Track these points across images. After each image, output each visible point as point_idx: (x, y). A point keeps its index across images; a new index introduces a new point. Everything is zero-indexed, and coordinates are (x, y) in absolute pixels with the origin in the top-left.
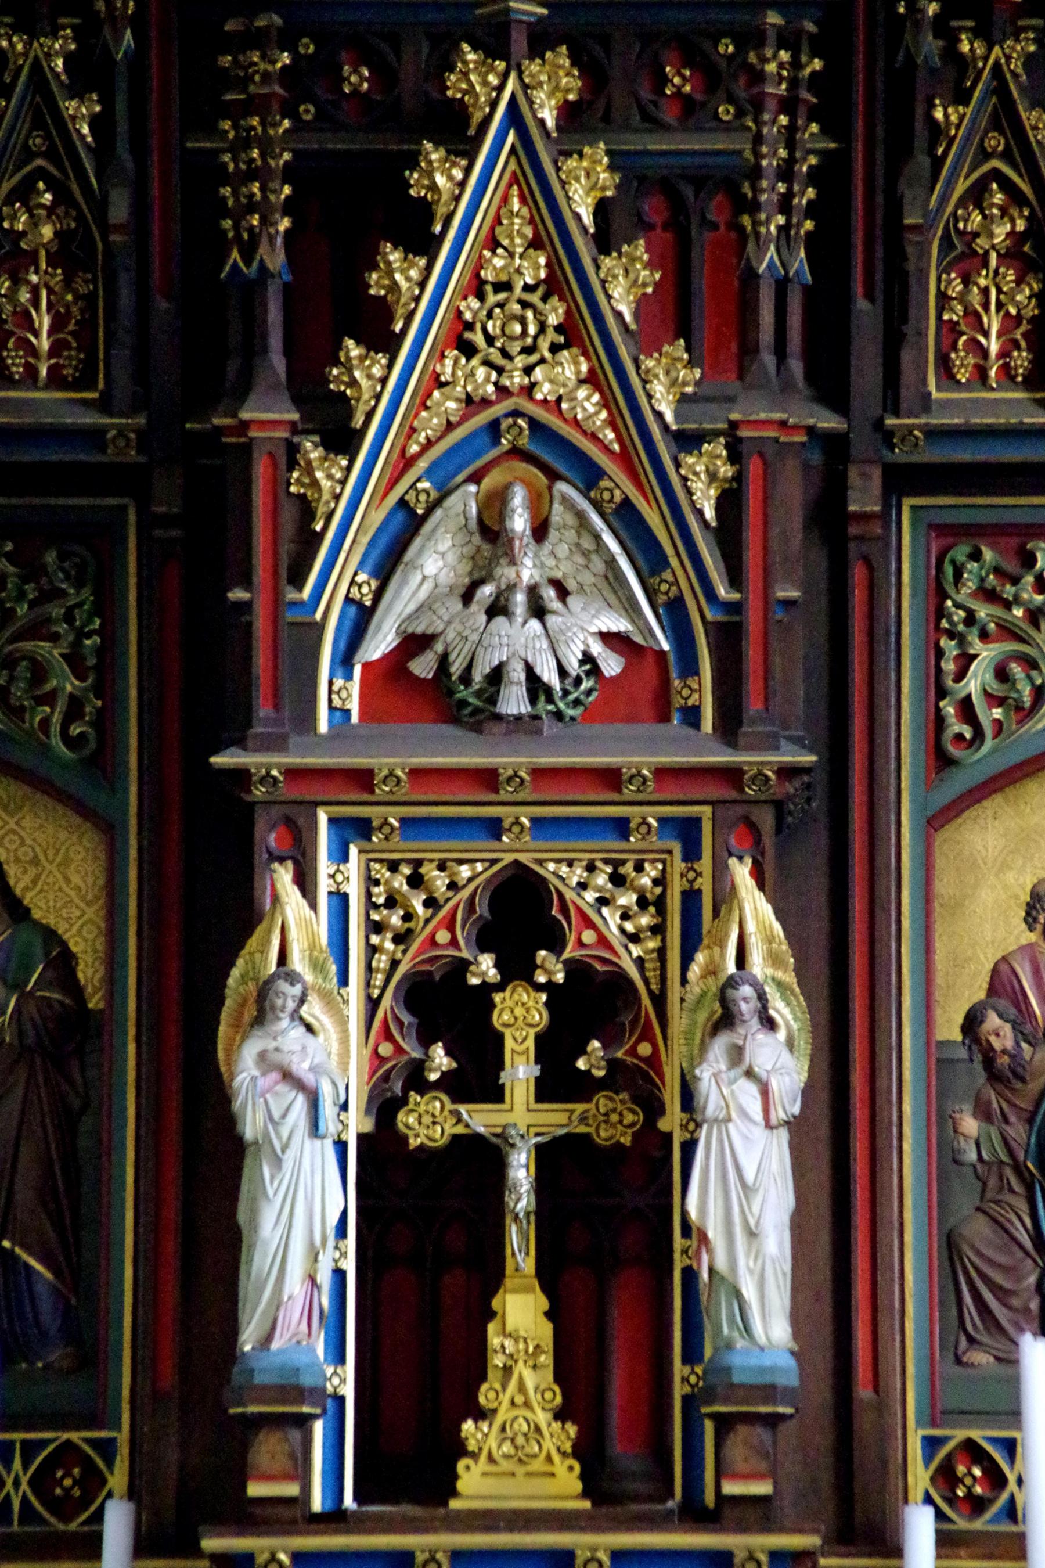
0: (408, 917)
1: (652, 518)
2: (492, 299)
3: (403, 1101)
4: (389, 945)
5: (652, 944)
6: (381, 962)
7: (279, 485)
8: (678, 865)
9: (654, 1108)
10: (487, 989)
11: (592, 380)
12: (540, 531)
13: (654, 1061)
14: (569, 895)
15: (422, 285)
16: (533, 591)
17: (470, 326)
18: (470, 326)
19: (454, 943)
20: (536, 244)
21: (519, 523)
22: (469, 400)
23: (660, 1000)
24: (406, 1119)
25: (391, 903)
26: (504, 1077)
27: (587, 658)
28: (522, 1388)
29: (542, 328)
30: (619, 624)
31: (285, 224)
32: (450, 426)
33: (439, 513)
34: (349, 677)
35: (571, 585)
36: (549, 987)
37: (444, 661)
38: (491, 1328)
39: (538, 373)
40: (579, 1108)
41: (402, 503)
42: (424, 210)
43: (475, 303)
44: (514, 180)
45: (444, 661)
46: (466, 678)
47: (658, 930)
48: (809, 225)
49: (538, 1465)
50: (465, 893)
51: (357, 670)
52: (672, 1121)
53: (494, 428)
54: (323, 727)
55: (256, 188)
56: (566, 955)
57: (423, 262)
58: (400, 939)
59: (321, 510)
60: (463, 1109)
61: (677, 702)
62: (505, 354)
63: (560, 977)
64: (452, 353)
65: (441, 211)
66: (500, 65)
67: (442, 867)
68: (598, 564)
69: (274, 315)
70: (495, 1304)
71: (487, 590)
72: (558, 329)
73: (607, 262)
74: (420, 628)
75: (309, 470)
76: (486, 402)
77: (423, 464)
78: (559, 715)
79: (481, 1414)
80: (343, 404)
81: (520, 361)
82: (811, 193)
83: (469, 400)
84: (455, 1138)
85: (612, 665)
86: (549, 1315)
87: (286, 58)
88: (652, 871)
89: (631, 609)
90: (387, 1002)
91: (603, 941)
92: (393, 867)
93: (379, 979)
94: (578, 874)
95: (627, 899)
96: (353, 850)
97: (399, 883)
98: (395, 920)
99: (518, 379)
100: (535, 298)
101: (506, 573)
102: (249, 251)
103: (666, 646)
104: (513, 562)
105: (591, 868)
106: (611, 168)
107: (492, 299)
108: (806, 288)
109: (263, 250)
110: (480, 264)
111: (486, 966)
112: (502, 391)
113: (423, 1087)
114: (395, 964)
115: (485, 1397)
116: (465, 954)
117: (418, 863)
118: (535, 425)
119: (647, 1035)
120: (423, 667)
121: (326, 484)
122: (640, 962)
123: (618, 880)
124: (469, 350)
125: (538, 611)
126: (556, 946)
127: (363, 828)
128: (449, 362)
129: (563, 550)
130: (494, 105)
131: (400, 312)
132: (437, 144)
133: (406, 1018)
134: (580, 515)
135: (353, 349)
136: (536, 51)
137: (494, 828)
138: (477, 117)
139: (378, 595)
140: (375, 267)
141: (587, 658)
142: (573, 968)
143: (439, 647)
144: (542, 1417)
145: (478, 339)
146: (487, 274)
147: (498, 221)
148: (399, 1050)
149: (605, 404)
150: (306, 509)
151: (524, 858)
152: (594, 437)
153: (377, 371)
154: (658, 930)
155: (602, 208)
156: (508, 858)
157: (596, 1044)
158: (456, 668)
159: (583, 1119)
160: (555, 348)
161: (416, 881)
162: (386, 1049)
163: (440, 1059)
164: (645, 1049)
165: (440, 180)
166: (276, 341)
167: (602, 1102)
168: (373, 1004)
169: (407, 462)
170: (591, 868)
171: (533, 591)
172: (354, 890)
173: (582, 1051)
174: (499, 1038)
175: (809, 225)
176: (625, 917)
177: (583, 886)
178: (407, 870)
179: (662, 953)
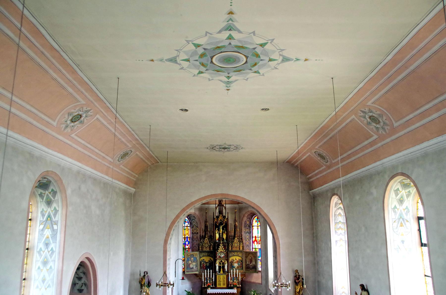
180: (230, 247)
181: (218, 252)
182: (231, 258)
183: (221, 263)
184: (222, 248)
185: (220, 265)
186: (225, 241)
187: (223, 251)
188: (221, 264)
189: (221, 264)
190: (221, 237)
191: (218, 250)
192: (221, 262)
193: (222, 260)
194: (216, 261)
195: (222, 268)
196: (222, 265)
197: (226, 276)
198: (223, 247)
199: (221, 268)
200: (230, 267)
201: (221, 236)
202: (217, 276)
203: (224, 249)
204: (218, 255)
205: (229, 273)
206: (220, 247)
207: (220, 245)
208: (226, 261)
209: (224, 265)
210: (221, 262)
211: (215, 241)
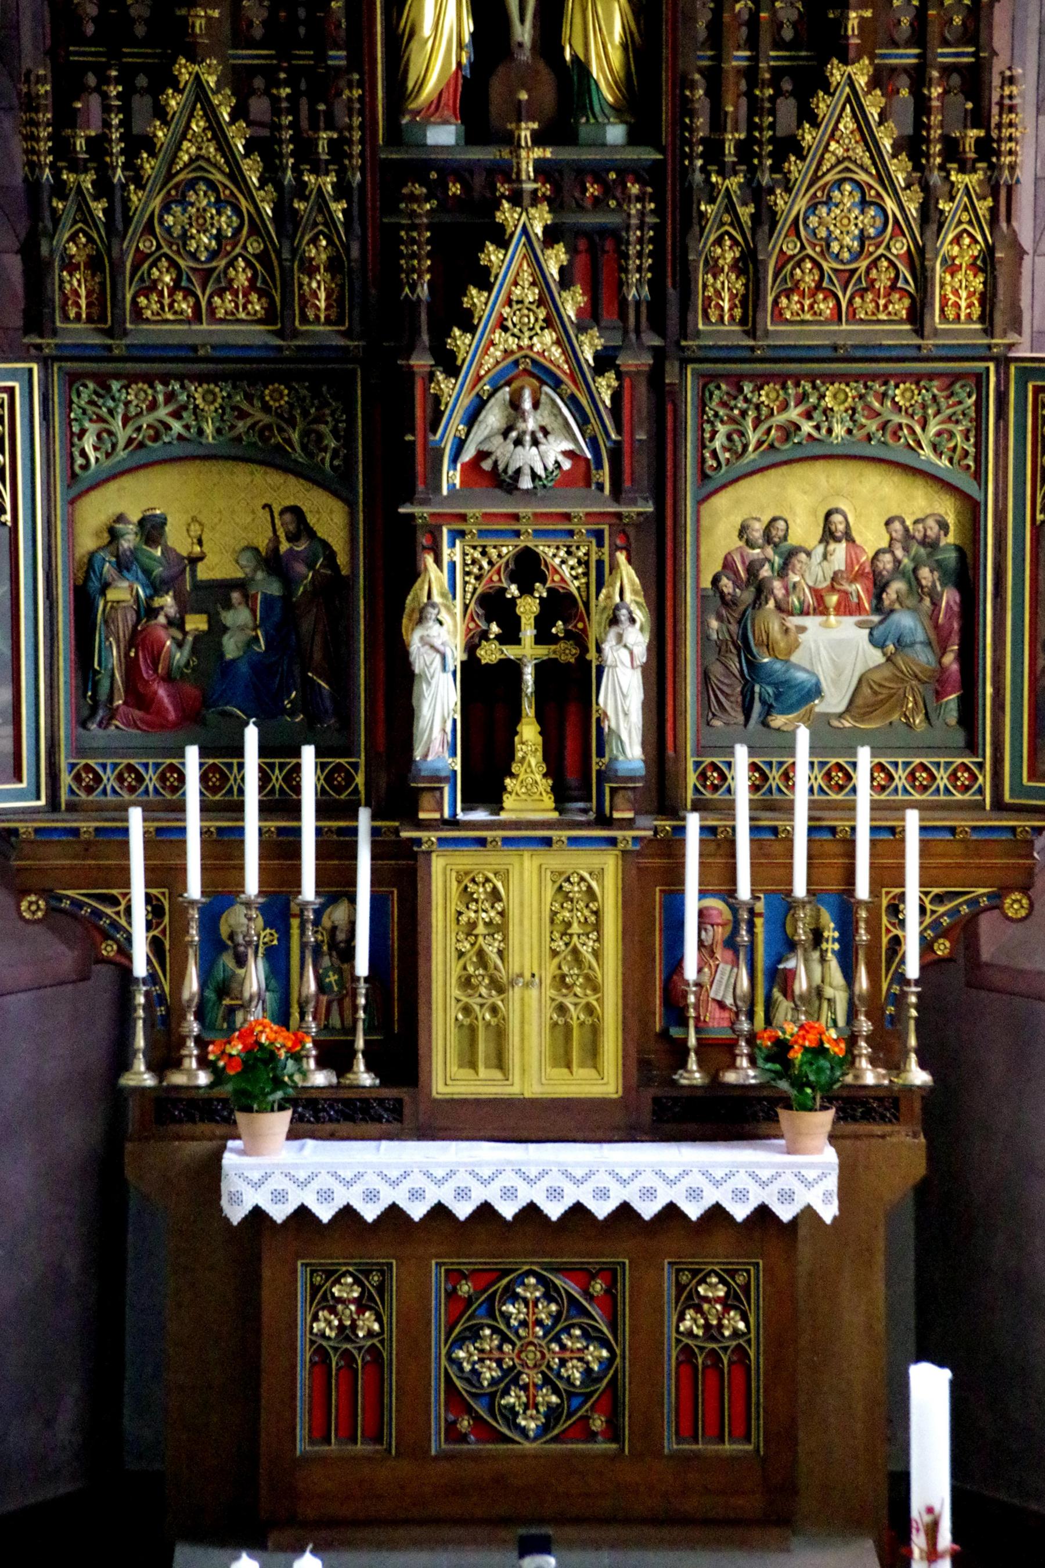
0: (481, 568)
1: (584, 401)
2: (515, 307)
3: (479, 645)
4: (473, 581)
5: (583, 580)
6: (470, 588)
7: (426, 389)
8: (594, 548)
9: (585, 650)
10: (514, 598)
11: (558, 342)
12: (536, 405)
13: (584, 630)
14: (549, 560)
15: (486, 304)
16: (533, 433)
17: (506, 319)
18: (506, 319)
19: (500, 580)
20: (533, 284)
21: (527, 405)
22: (505, 351)
23: (587, 604)
24: (480, 653)
25: (474, 562)
26: (521, 635)
27: (557, 462)
28: (530, 765)
29: (536, 320)
30: (569, 446)
31: (428, 277)
32: (498, 363)
33: (493, 400)
34: (455, 469)
35: (549, 428)
36: (541, 598)
37: (496, 463)
38: (517, 739)
39: (535, 339)
40: (553, 647)
41: (478, 395)
42: (487, 270)
43: (507, 309)
44: (525, 256)
45: (496, 463)
46: (505, 471)
47: (586, 574)
48: (649, 275)
49: (536, 797)
50: (504, 560)
51: (459, 466)
52: (592, 655)
53: (516, 363)
54: (445, 492)
55: (415, 262)
56: (548, 585)
57: (486, 294)
58: (478, 578)
59: (444, 401)
60: (504, 648)
61: (594, 480)
62: (520, 330)
63: (545, 595)
64: (498, 331)
65: (494, 272)
66: (518, 210)
67: (495, 547)
68: (560, 420)
69: (424, 317)
70: (518, 729)
71: (514, 434)
72: (544, 320)
73: (564, 294)
74: (485, 448)
75: (438, 383)
76: (512, 352)
77: (486, 379)
78: (544, 486)
79: (512, 776)
80: (453, 355)
81: (527, 334)
82: (650, 261)
83: (505, 351)
84: (501, 660)
85: (567, 465)
86: (541, 733)
87: (428, 206)
88: (583, 550)
89: (575, 440)
90: (472, 606)
91: (563, 580)
92: (474, 548)
93: (469, 596)
94: (553, 551)
95: (572, 562)
96: (458, 542)
97: (477, 555)
98: (475, 570)
99: (526, 342)
100: (534, 307)
101: (521, 426)
102: (413, 288)
103: (589, 456)
104: (525, 421)
105: (558, 548)
106: (566, 253)
107: (515, 307)
108: (648, 302)
109: (419, 289)
110: (510, 293)
111: (514, 590)
112: (520, 347)
113: (487, 639)
114: (475, 589)
115: (515, 769)
116: (505, 585)
117: (484, 547)
118: (534, 362)
119: (582, 620)
120: (487, 465)
121: (446, 390)
122: (578, 588)
123: (569, 553)
124: (505, 329)
125: (535, 443)
126: (544, 582)
127: (462, 534)
128: (497, 335)
129: (546, 413)
130: (516, 226)
131: (476, 315)
132: (492, 243)
133: (481, 612)
134: (553, 401)
135: (457, 332)
136: (534, 204)
137: (517, 534)
138: (509, 231)
139: (467, 435)
140: (465, 295)
141: (557, 462)
142: (550, 590)
143: (493, 458)
144: (538, 777)
145: (509, 324)
146: (514, 298)
147: (518, 274)
148: (477, 626)
149: (564, 353)
150: (437, 399)
151: (530, 544)
152: (558, 367)
153: (467, 342)
154: (586, 574)
155: (562, 270)
156: (522, 545)
157: (560, 623)
158: (501, 467)
159: (554, 652)
160: (542, 329)
161: (484, 553)
162: (472, 625)
163: (495, 628)
164: (580, 625)
165: (493, 258)
166: (424, 327)
167: (562, 645)
168: (466, 607)
169: (480, 378)
170: (558, 548)
171: (533, 433)
172: (458, 559)
173: (554, 625)
174: (518, 619)
175: (649, 275)
176: (572, 568)
177: (554, 556)
178: (480, 549)
179: (587, 584)
180: (715, 269)
181: (453, 371)
182: (721, 501)
183: (528, 609)
184: (540, 278)
185: (490, 653)
186: (615, 133)
187: (572, 354)
188: (528, 632)
189: (528, 632)
190: (525, 56)
191: (460, 341)
192: (526, 590)
193: (545, 550)
194: (413, 573)
195: (528, 710)
196: (543, 637)
197: (609, 862)
198: (555, 260)
199: (516, 717)
200: (705, 677)
201: (524, 33)
202: (438, 864)
203: (590, 317)
204: (453, 426)
205: (693, 822)
206: (492, 255)
207: (507, 215)
208: (628, 574)
209: (579, 639)
210: (526, 590)
211: (396, 135)
